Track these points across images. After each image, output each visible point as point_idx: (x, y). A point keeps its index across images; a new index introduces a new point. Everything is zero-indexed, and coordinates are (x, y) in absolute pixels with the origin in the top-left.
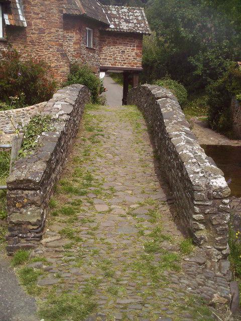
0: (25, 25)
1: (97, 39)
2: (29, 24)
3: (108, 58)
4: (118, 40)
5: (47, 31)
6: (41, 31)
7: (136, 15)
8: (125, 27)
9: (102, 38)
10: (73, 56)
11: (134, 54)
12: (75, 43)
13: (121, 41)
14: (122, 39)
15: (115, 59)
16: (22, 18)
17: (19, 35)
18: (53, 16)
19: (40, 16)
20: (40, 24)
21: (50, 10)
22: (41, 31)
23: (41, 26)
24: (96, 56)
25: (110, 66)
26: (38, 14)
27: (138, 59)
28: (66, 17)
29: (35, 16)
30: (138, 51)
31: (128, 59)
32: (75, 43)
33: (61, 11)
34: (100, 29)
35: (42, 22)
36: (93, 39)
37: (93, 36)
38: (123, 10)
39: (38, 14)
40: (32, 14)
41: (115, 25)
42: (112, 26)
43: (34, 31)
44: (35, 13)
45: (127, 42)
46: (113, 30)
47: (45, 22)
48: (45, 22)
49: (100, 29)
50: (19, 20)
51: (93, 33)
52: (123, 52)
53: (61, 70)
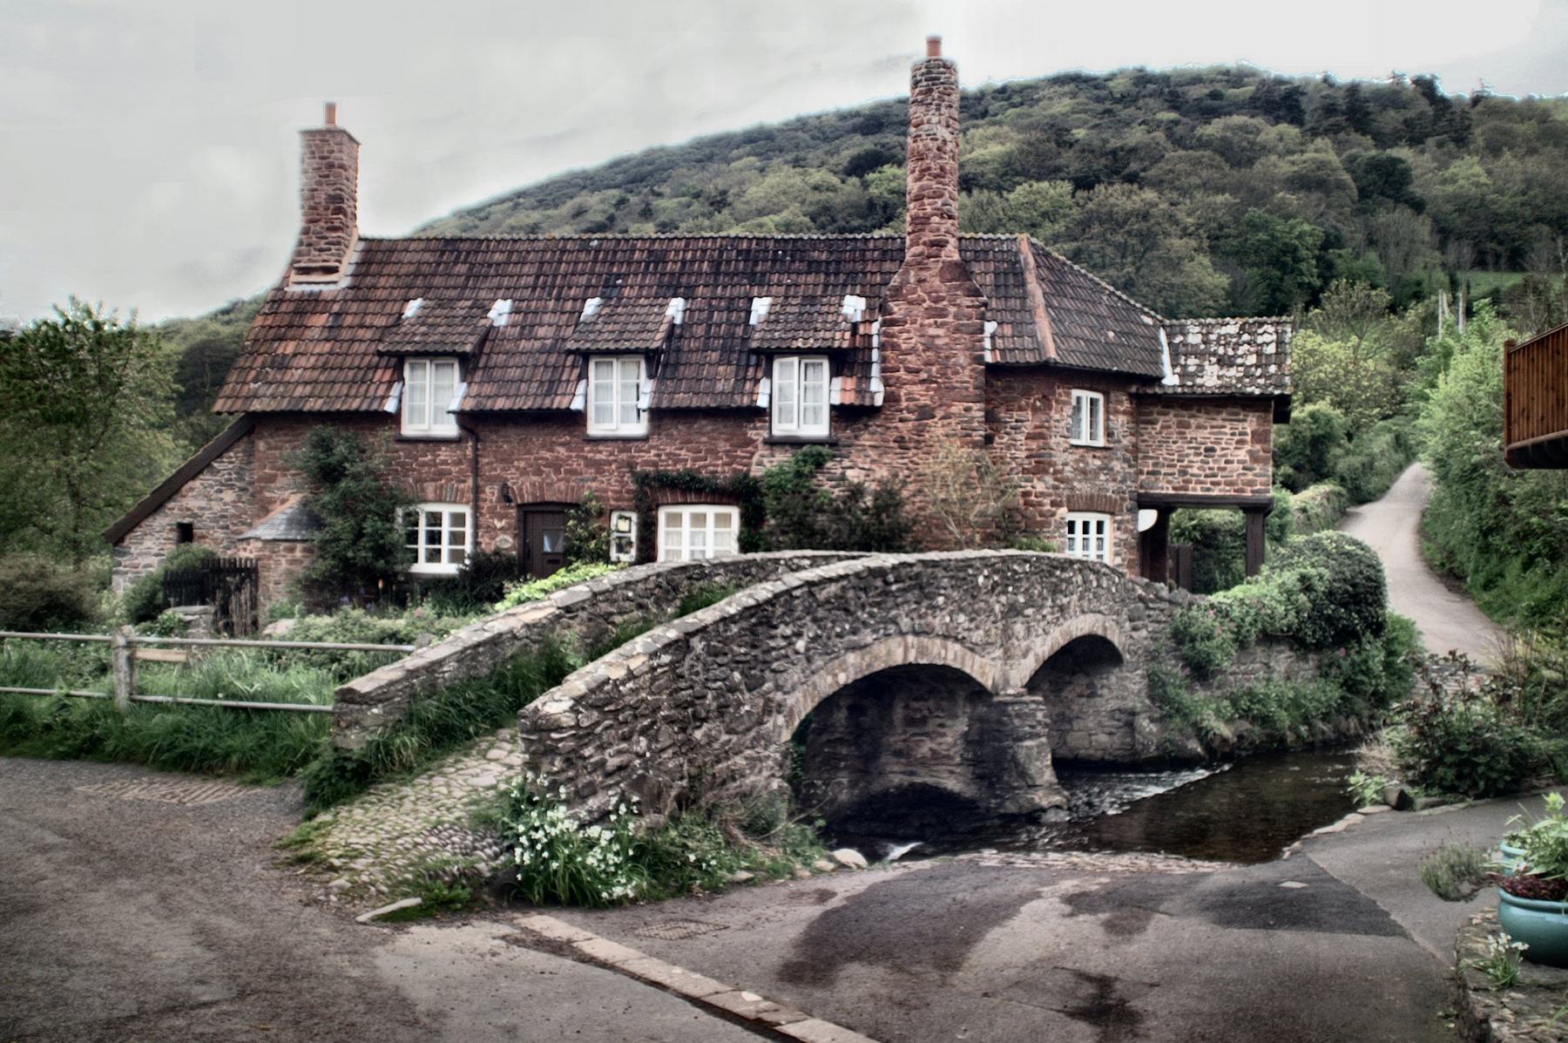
0: (879, 401)
1: (1122, 419)
2: (891, 398)
3: (1163, 471)
4: (1193, 416)
5: (939, 413)
6: (925, 413)
7: (1260, 340)
8: (1212, 379)
9: (1141, 414)
10: (1025, 471)
11: (1242, 454)
12: (1029, 437)
13: (1202, 420)
14: (1207, 413)
15: (1183, 472)
16: (876, 385)
17: (867, 426)
18: (957, 373)
19: (924, 376)
20: (922, 395)
21: (947, 358)
22: (925, 413)
23: (924, 401)
24: (1117, 466)
25: (1171, 492)
26: (918, 371)
27: (1258, 468)
28: (993, 370)
29: (909, 377)
30: (1258, 447)
31: (1224, 469)
32: (1029, 437)
33: (979, 359)
34: (1133, 389)
35: (927, 390)
36: (1107, 420)
37: (1107, 412)
38: (1224, 330)
39: (918, 371)
40: (902, 373)
41: (1184, 375)
42: (1171, 379)
43: (906, 415)
44: (909, 371)
45: (1220, 423)
46: (1170, 391)
47: (935, 390)
48: (935, 390)
49: (1133, 389)
50: (867, 391)
51: (1107, 402)
52: (1210, 450)
53: (978, 508)
